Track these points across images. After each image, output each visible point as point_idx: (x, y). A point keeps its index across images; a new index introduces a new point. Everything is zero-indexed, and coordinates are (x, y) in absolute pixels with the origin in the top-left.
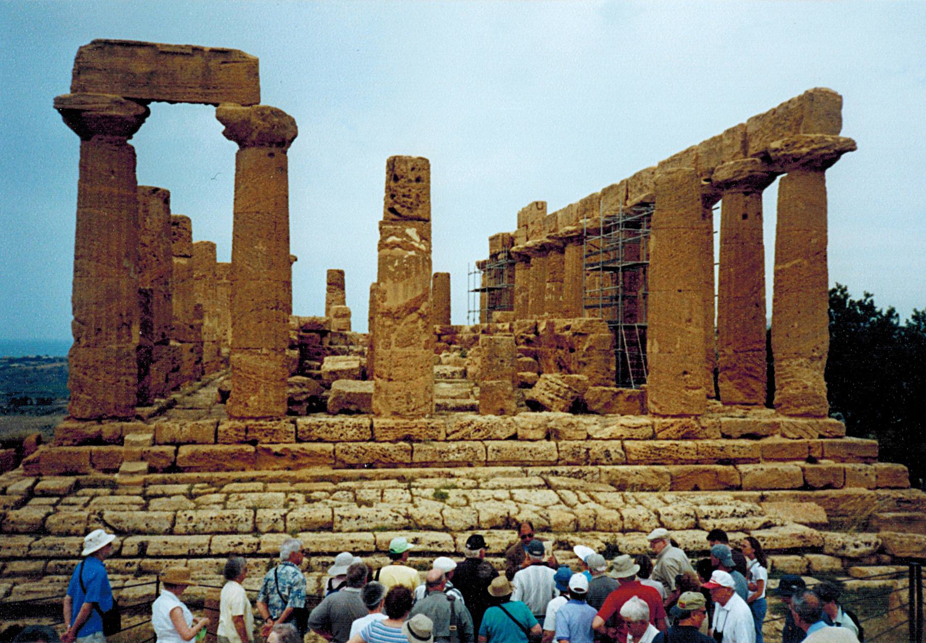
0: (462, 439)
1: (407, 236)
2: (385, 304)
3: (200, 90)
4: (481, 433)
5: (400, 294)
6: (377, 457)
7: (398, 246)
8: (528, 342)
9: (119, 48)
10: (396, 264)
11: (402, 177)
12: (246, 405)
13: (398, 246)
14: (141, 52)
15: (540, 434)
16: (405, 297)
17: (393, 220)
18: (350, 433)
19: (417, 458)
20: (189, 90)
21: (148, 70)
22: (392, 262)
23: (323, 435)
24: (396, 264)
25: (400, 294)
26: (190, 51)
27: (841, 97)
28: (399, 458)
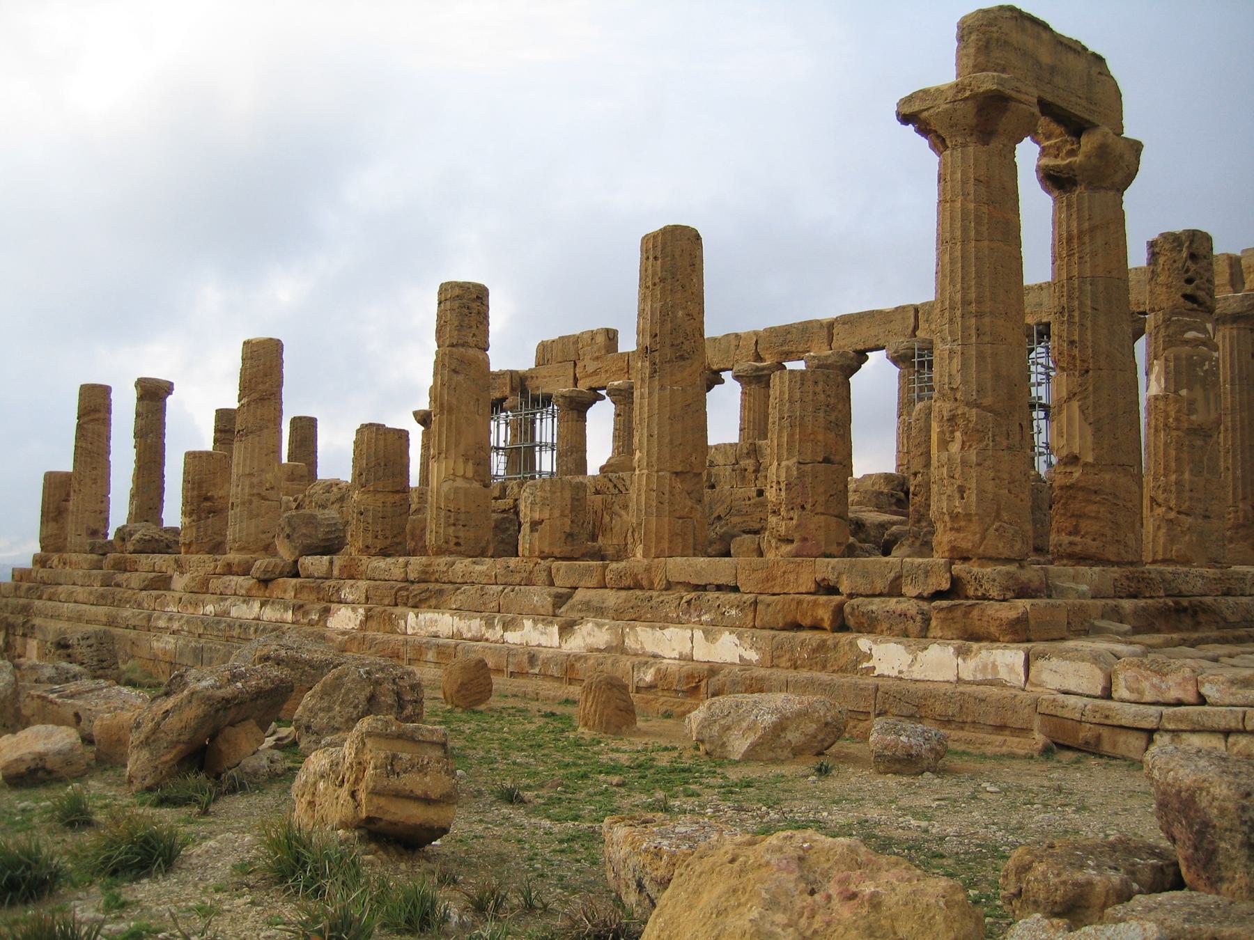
2: (1194, 417)
3: (1084, 103)
7: (1204, 343)
9: (1028, 24)
10: (1206, 367)
12: (1126, 545)
13: (1204, 343)
14: (1045, 36)
17: (1192, 310)
23: (1184, 587)
24: (1206, 367)
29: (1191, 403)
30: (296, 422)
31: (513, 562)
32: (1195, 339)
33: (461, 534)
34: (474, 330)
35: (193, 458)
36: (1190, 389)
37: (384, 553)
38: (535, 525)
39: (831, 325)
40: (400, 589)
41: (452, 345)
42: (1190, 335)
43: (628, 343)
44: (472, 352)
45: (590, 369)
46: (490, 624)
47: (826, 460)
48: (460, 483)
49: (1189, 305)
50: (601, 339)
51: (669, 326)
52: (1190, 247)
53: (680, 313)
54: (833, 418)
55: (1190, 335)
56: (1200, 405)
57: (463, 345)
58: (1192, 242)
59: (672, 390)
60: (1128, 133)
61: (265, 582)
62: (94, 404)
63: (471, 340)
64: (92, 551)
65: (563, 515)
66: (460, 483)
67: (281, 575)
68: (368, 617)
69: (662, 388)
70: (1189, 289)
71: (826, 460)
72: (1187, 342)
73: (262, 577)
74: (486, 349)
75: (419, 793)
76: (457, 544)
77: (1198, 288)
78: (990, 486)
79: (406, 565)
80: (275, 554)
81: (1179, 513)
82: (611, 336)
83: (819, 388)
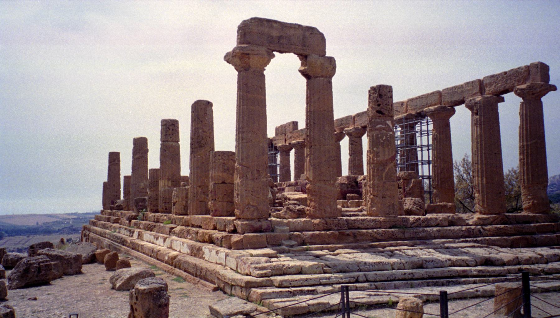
0: (417, 227)
1: (388, 125)
2: (379, 159)
4: (425, 223)
5: (387, 153)
6: (390, 236)
8: (352, 186)
11: (385, 95)
12: (325, 211)
14: (275, 25)
15: (447, 224)
16: (389, 155)
18: (372, 224)
19: (407, 235)
20: (297, 47)
21: (278, 35)
22: (382, 138)
23: (360, 226)
24: (384, 138)
25: (387, 153)
26: (297, 27)
27: (548, 66)
28: (399, 236)
29: (378, 153)
32: (380, 128)
34: (171, 135)
35: (126, 177)
36: (377, 148)
39: (354, 117)
42: (378, 126)
43: (302, 125)
44: (174, 144)
45: (289, 137)
46: (154, 238)
47: (223, 183)
49: (379, 115)
50: (291, 125)
51: (196, 136)
52: (379, 92)
53: (200, 131)
54: (226, 168)
55: (378, 126)
56: (381, 154)
57: (167, 141)
58: (379, 90)
60: (328, 55)
63: (170, 140)
66: (167, 188)
69: (195, 157)
70: (378, 108)
71: (223, 183)
72: (376, 130)
74: (178, 141)
76: (166, 209)
77: (382, 108)
78: (244, 194)
81: (374, 196)
82: (295, 124)
83: (220, 158)
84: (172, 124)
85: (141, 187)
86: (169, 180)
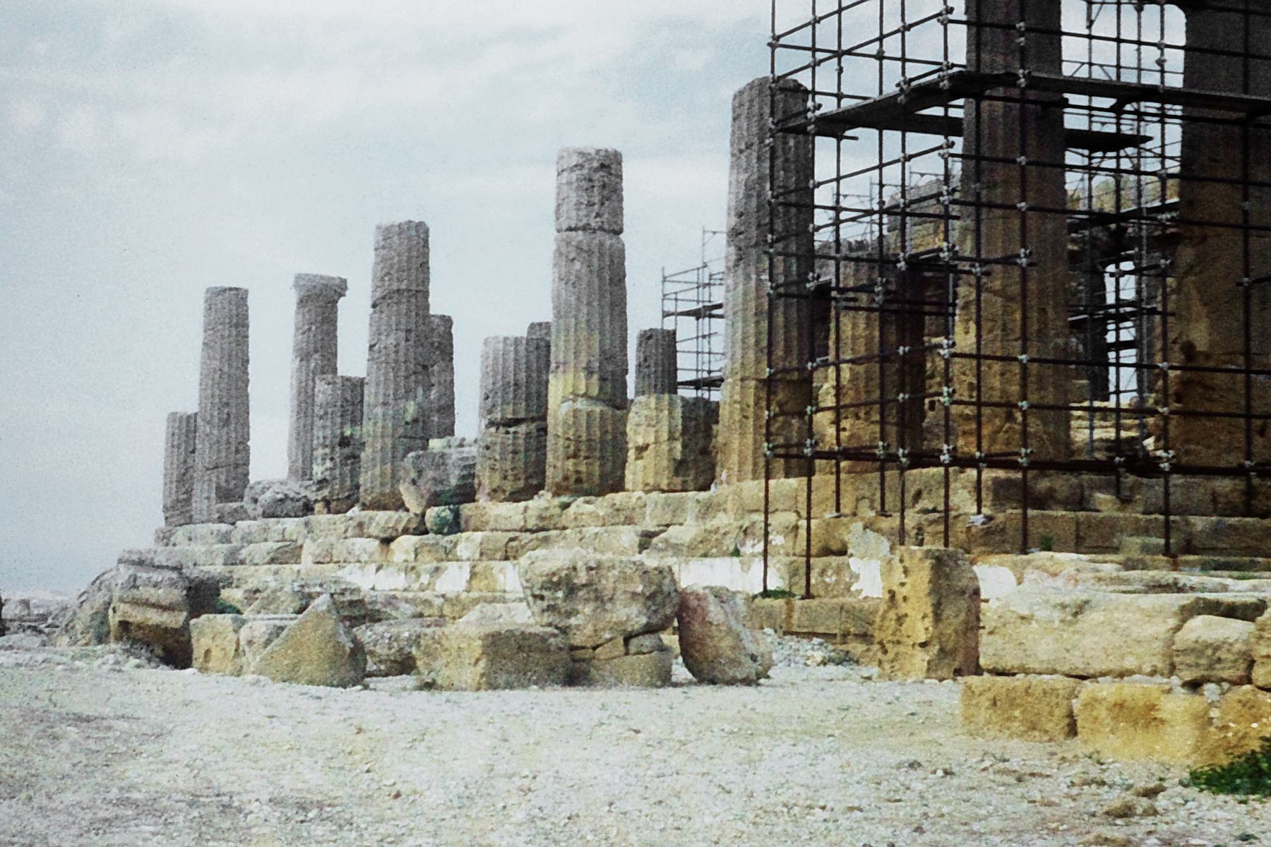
30: (646, 337)
31: (618, 497)
33: (583, 468)
37: (515, 497)
38: (641, 449)
40: (512, 540)
41: (570, 229)
48: (581, 404)
59: (759, 281)
61: (387, 541)
62: (230, 316)
64: (221, 520)
65: (671, 438)
67: (406, 531)
68: (473, 575)
69: (748, 277)
73: (382, 535)
75: (153, 600)
76: (579, 481)
79: (526, 509)
80: (401, 506)
84: (603, 166)
85: (409, 419)
86: (589, 372)
